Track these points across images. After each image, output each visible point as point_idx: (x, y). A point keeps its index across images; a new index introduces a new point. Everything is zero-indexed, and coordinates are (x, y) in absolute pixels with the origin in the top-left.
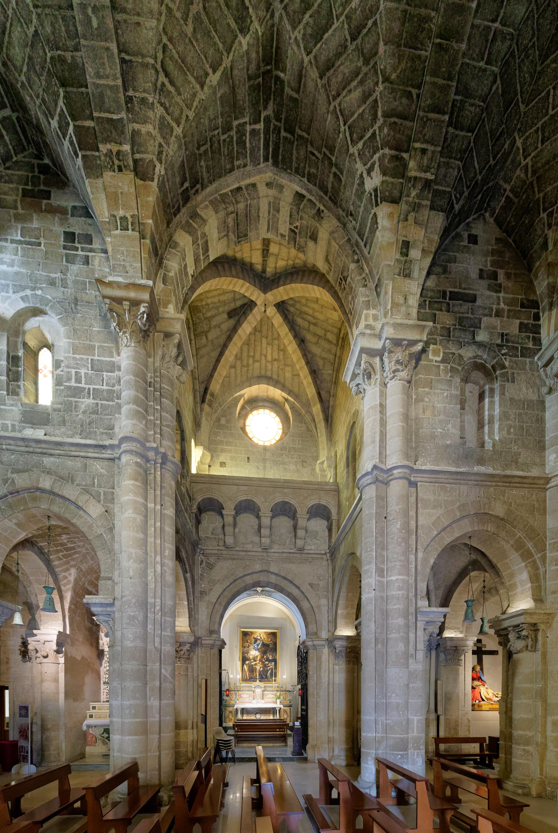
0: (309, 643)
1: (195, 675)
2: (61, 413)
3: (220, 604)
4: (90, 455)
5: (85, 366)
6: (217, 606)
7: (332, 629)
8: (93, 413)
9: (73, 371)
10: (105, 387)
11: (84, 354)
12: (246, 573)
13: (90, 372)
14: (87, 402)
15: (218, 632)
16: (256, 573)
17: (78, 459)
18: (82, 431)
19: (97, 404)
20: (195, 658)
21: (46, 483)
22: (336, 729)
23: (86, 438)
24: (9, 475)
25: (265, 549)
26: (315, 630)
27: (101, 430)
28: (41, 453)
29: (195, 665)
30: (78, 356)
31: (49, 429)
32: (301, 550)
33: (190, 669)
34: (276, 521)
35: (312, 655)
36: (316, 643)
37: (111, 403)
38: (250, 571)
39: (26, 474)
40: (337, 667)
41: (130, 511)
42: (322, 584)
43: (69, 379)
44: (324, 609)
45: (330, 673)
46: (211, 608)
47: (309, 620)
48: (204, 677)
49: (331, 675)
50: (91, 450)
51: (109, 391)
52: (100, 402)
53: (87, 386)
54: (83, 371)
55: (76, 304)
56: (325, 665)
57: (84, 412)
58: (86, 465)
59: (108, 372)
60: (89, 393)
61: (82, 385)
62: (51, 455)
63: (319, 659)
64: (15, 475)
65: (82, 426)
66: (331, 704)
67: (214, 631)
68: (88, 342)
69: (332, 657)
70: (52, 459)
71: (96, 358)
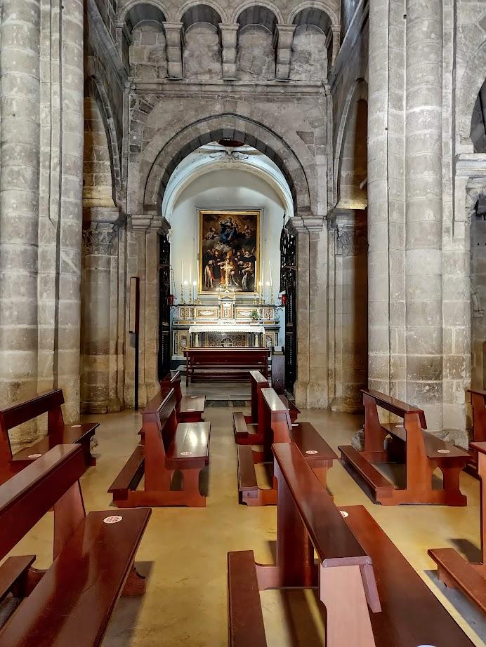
0: (298, 223)
1: (121, 271)
3: (161, 165)
6: (156, 167)
7: (333, 201)
12: (199, 118)
15: (159, 209)
16: (216, 116)
20: (121, 245)
22: (340, 356)
25: (229, 82)
26: (307, 204)
29: (122, 257)
32: (285, 81)
33: (113, 263)
34: (245, 39)
35: (302, 242)
36: (307, 222)
38: (207, 115)
40: (340, 259)
42: (318, 132)
44: (321, 171)
45: (328, 263)
46: (147, 170)
47: (297, 188)
48: (135, 275)
49: (332, 273)
56: (322, 258)
63: (313, 247)
66: (331, 317)
67: (152, 207)
69: (332, 245)
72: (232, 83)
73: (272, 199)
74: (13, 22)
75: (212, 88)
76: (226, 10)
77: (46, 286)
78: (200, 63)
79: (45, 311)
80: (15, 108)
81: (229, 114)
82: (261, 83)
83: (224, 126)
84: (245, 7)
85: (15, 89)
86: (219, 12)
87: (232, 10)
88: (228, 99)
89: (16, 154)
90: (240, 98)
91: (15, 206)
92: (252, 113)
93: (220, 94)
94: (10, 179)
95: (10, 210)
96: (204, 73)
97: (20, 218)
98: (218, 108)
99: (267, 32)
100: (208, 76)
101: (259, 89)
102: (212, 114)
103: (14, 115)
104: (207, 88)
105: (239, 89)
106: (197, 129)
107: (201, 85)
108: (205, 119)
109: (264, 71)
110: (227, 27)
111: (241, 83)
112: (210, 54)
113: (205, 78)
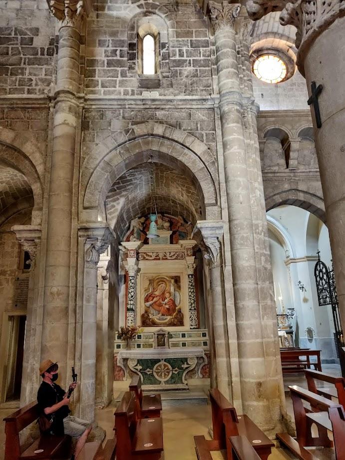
2: (168, 79)
4: (194, 107)
5: (185, 45)
8: (194, 77)
9: (177, 49)
10: (202, 58)
11: (184, 37)
13: (190, 48)
14: (188, 70)
17: (183, 110)
18: (186, 90)
19: (197, 70)
21: (159, 130)
23: (189, 95)
24: (130, 126)
27: (201, 88)
28: (155, 108)
30: (180, 39)
31: (161, 90)
37: (207, 68)
39: (143, 124)
41: (236, 147)
43: (174, 55)
50: (194, 103)
51: (204, 60)
52: (198, 69)
53: (188, 59)
54: (184, 49)
55: (177, 6)
57: (187, 77)
58: (190, 114)
59: (203, 47)
60: (190, 63)
61: (185, 58)
62: (162, 109)
64: (134, 127)
65: (186, 86)
68: (188, 29)
70: (163, 112)
71: (194, 39)
72: (295, 171)
73: (272, 239)
74: (236, 151)
75: (283, 175)
76: (292, 131)
77: (265, 311)
78: (271, 160)
79: (266, 328)
80: (241, 199)
81: (293, 189)
82: (313, 170)
83: (290, 197)
84: (302, 129)
85: (241, 188)
86: (287, 132)
87: (295, 131)
88: (292, 181)
89: (245, 226)
90: (299, 180)
91: (247, 259)
92: (308, 188)
93: (287, 178)
94: (242, 242)
95: (244, 262)
96: (275, 166)
97: (250, 266)
98: (286, 186)
99: (310, 140)
100: (277, 167)
101: (311, 174)
102: (284, 190)
103: (241, 203)
104: (278, 174)
105: (299, 174)
106: (273, 200)
107: (275, 173)
108: (278, 194)
109: (312, 163)
110: (295, 140)
111: (300, 171)
112: (277, 155)
113: (276, 168)
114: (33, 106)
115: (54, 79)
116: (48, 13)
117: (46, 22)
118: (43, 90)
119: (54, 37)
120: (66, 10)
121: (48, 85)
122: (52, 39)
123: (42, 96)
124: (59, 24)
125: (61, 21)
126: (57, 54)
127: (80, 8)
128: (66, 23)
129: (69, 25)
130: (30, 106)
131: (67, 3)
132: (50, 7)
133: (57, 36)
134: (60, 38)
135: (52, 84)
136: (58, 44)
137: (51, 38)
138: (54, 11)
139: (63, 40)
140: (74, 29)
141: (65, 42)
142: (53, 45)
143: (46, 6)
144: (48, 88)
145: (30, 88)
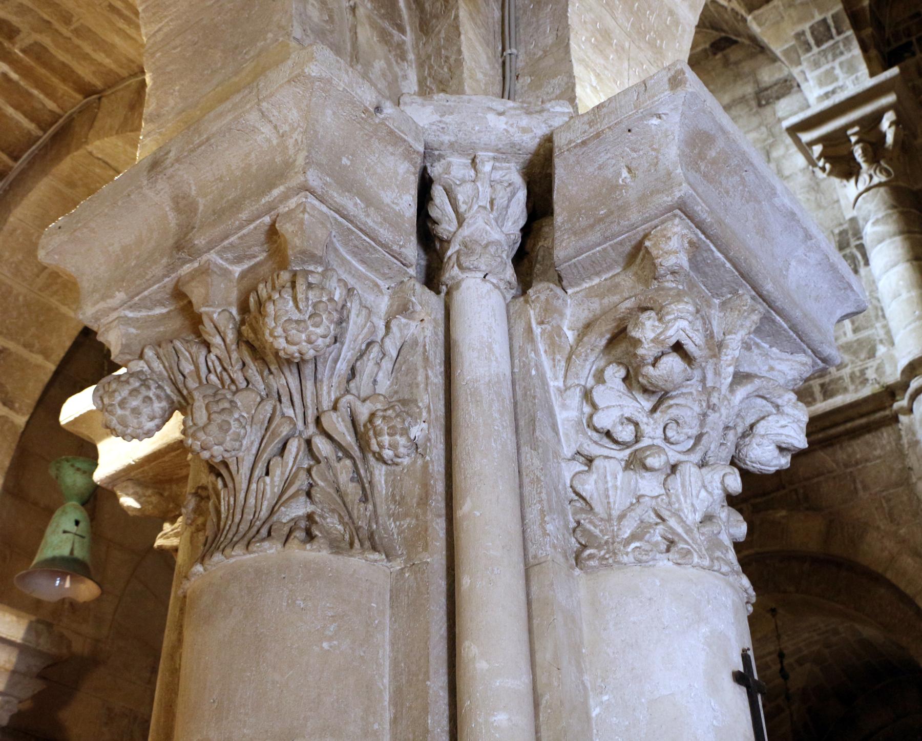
114: (849, 425)
115: (881, 333)
116: (809, 175)
117: (813, 198)
118: (863, 372)
119: (846, 226)
120: (858, 152)
121: (872, 354)
122: (841, 233)
123: (866, 392)
124: (850, 189)
125: (853, 181)
126: (867, 263)
127: (893, 128)
128: (868, 178)
129: (876, 180)
130: (841, 428)
131: (854, 134)
132: (812, 162)
133: (853, 220)
134: (861, 222)
135: (881, 350)
136: (861, 238)
137: (837, 231)
138: (828, 166)
139: (874, 224)
140: (894, 183)
141: (880, 228)
142: (848, 245)
143: (800, 160)
144: (873, 363)
145: (827, 379)
